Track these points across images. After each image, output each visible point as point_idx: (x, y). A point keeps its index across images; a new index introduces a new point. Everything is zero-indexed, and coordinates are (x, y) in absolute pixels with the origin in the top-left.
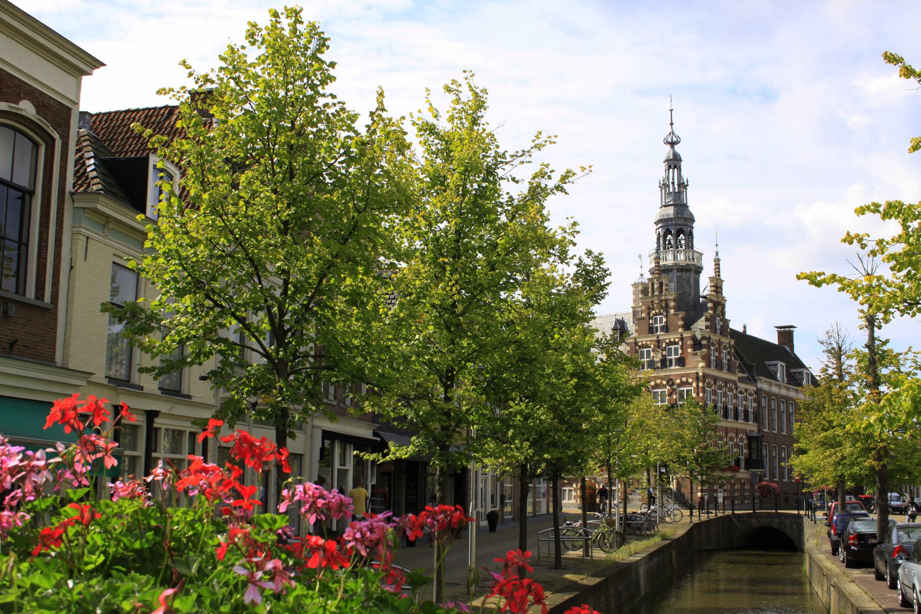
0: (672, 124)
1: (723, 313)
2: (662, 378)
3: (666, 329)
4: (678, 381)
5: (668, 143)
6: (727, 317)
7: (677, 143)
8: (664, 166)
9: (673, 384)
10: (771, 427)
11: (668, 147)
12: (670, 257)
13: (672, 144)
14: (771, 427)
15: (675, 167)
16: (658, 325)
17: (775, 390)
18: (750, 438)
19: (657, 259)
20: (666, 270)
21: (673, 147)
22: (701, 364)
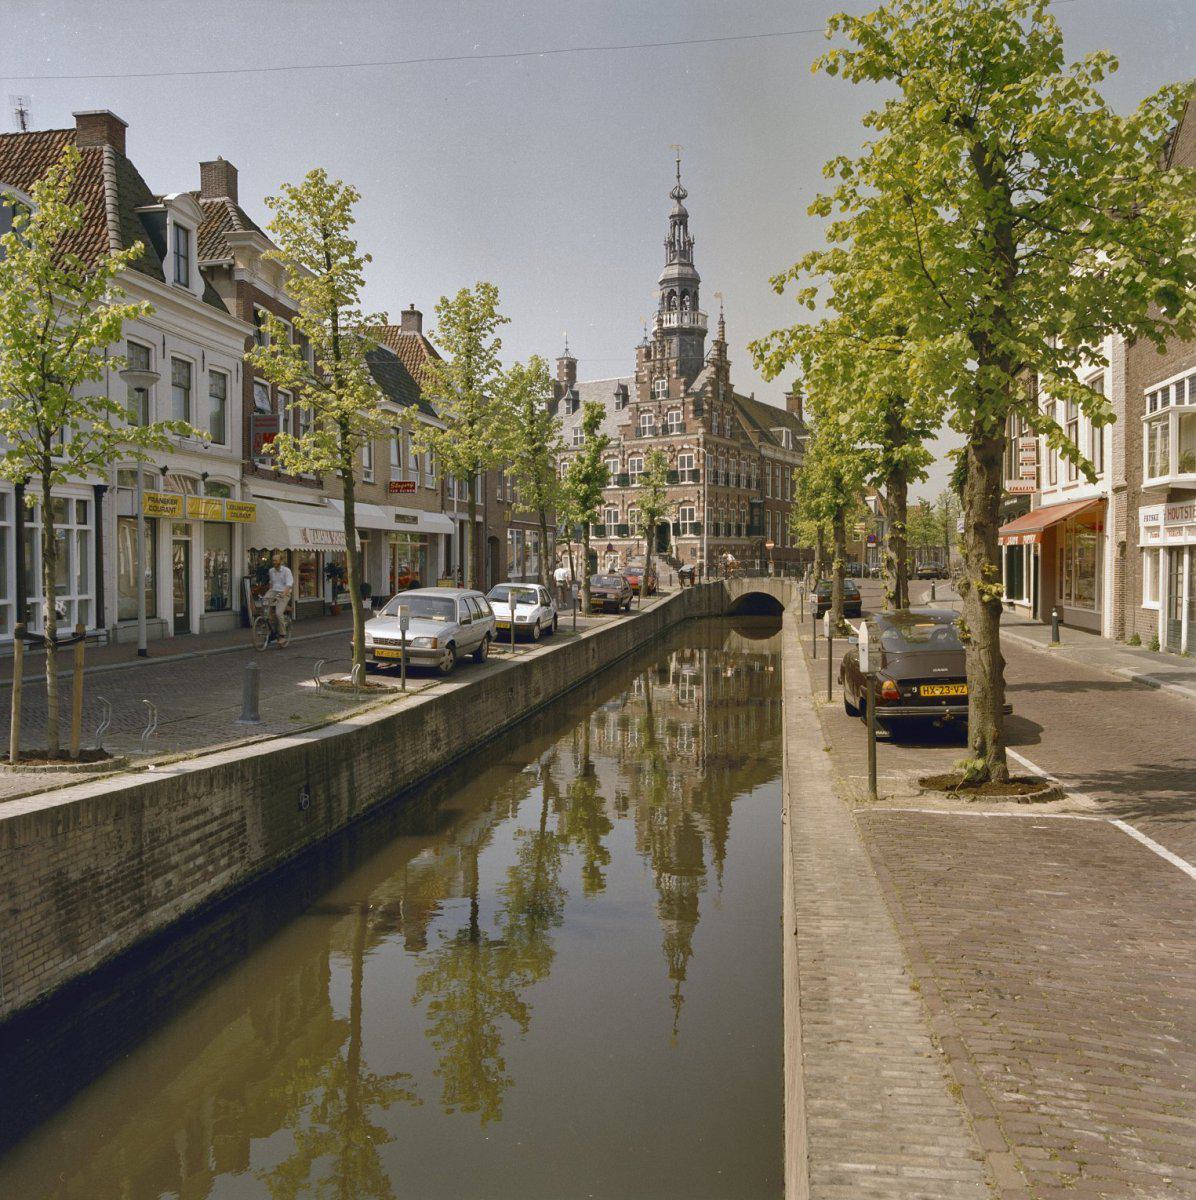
0: (679, 177)
1: (727, 378)
2: (664, 444)
3: (667, 394)
4: (679, 447)
5: (674, 197)
6: (731, 382)
7: (685, 196)
8: (668, 222)
9: (674, 450)
10: (774, 494)
11: (675, 201)
12: (674, 317)
13: (679, 198)
14: (774, 494)
15: (681, 224)
16: (661, 390)
17: (779, 456)
18: (752, 506)
19: (660, 321)
20: (670, 332)
21: (679, 202)
22: (701, 431)
